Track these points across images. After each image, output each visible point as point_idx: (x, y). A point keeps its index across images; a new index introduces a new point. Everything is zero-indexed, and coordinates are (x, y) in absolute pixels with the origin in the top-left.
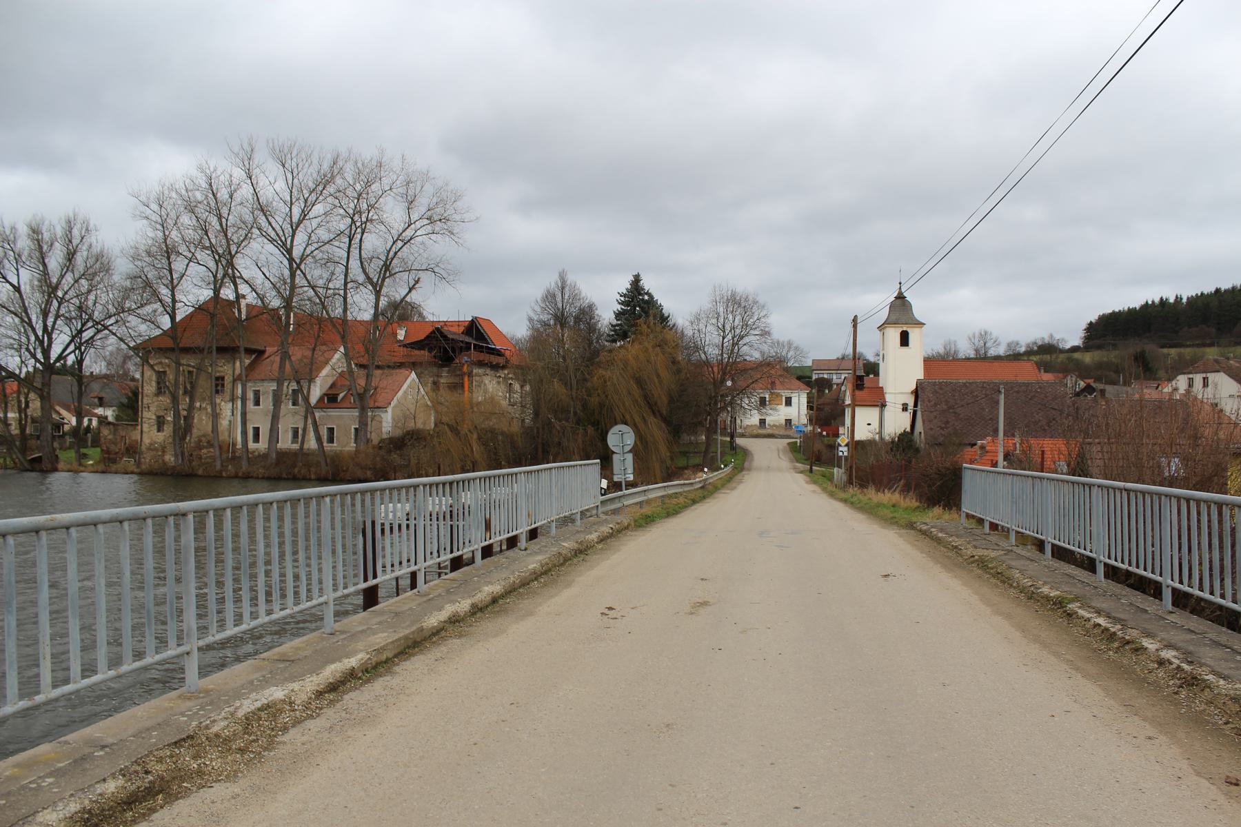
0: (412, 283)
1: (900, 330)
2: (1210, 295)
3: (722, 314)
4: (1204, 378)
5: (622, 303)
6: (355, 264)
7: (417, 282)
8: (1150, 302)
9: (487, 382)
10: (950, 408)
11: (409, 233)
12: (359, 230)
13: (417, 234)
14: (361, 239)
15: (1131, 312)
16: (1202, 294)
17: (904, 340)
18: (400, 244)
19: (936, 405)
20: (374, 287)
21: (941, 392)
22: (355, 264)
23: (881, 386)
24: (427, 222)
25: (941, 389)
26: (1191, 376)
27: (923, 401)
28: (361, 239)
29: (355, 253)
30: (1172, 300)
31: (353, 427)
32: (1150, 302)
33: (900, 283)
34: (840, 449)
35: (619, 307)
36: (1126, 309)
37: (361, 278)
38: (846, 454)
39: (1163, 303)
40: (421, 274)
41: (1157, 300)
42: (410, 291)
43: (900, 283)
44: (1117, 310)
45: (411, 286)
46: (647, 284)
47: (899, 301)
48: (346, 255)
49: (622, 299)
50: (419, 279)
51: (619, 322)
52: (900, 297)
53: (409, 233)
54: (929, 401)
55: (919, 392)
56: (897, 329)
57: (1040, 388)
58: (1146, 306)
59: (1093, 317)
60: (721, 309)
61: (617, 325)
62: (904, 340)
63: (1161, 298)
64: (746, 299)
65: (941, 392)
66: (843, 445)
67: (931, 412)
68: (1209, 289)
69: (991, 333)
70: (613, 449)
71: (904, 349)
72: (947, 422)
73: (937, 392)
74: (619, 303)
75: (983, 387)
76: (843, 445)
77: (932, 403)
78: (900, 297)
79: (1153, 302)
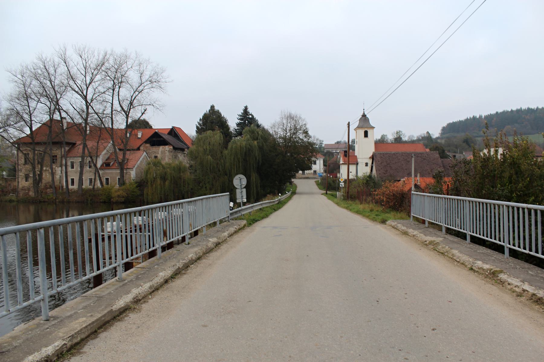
0: (143, 111)
1: (364, 130)
3: (285, 123)
5: (240, 119)
6: (116, 103)
7: (145, 110)
8: (469, 118)
9: (179, 156)
10: (388, 164)
11: (141, 88)
12: (117, 87)
13: (145, 88)
14: (119, 91)
15: (460, 122)
17: (366, 135)
18: (137, 93)
19: (381, 163)
20: (126, 114)
21: (384, 157)
22: (116, 103)
23: (356, 155)
24: (149, 82)
25: (384, 156)
27: (376, 161)
28: (119, 91)
29: (116, 98)
30: (478, 117)
31: (118, 177)
32: (469, 118)
34: (341, 184)
35: (239, 121)
36: (458, 120)
37: (119, 109)
38: (343, 186)
39: (474, 118)
40: (147, 107)
41: (472, 117)
42: (142, 114)
44: (455, 121)
45: (143, 112)
46: (250, 110)
47: (364, 118)
48: (111, 98)
49: (240, 117)
50: (146, 109)
51: (238, 128)
52: (364, 116)
53: (141, 88)
54: (379, 161)
55: (374, 158)
57: (427, 155)
58: (467, 120)
59: (445, 125)
60: (285, 121)
61: (238, 129)
62: (366, 135)
63: (474, 116)
64: (296, 117)
65: (384, 157)
66: (342, 182)
67: (380, 166)
68: (493, 112)
69: (402, 132)
70: (236, 186)
71: (366, 139)
72: (387, 171)
73: (382, 157)
74: (238, 119)
75: (402, 155)
77: (380, 162)
78: (364, 116)
79: (470, 118)
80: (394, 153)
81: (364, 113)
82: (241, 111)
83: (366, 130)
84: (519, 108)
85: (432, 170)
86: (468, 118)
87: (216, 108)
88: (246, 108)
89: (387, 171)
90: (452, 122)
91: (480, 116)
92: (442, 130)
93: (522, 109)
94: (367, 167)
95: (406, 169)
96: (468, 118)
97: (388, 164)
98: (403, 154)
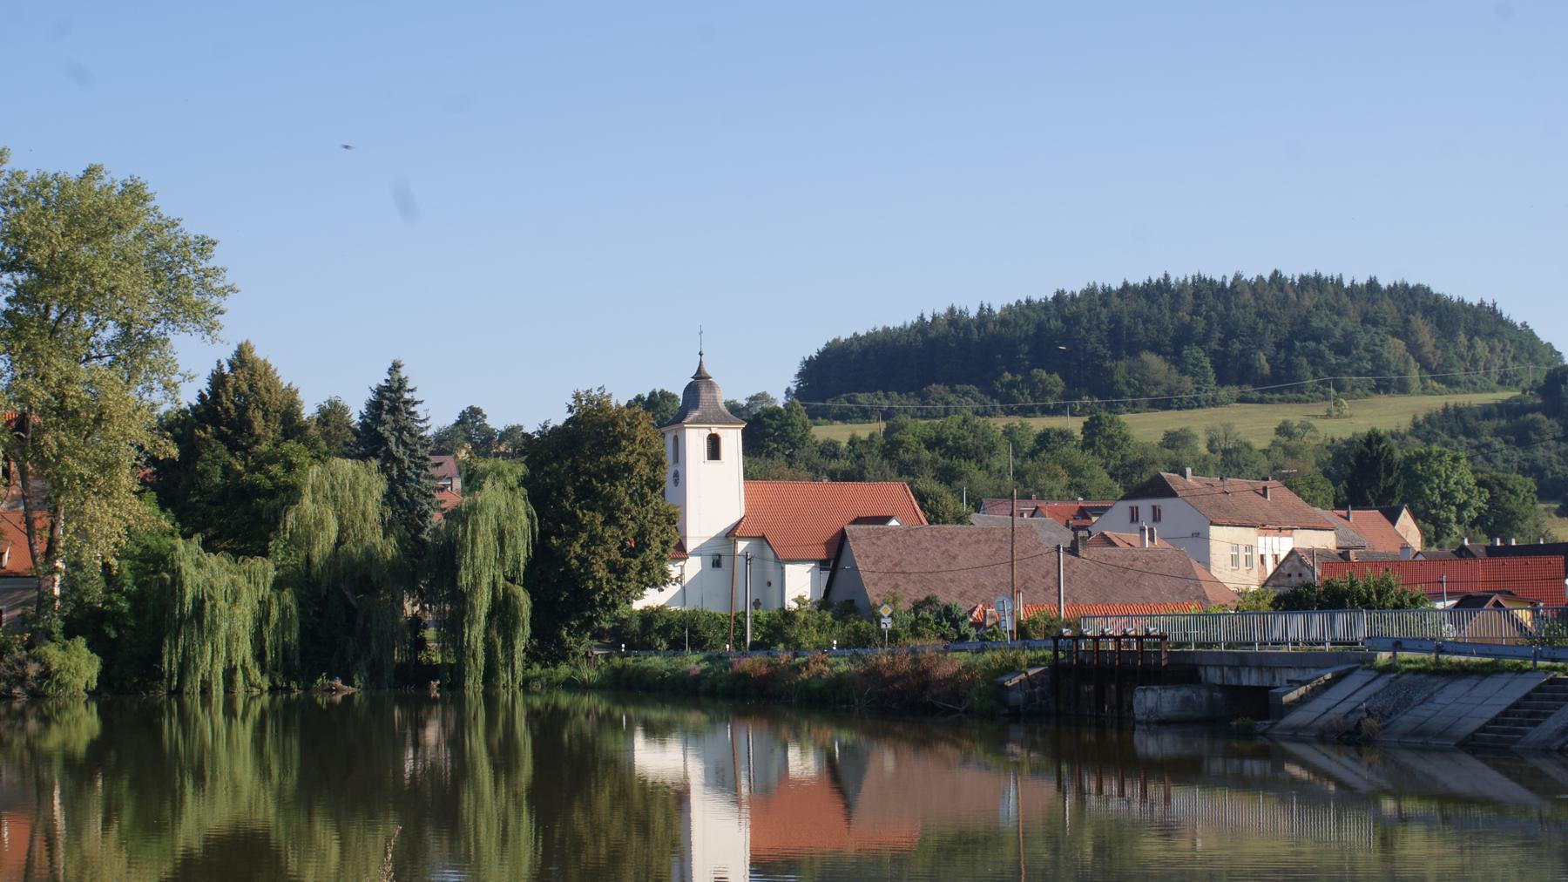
1: (707, 433)
2: (1045, 306)
4: (1154, 507)
8: (929, 319)
10: (896, 565)
16: (1028, 301)
19: (875, 563)
21: (879, 543)
26: (1134, 503)
30: (973, 313)
32: (929, 319)
33: (701, 354)
34: (883, 621)
36: (880, 329)
39: (954, 319)
41: (942, 310)
43: (701, 354)
44: (862, 333)
52: (700, 376)
54: (868, 557)
58: (921, 327)
59: (813, 348)
63: (952, 310)
65: (879, 543)
66: (886, 615)
68: (1042, 292)
73: (874, 544)
75: (932, 536)
76: (886, 615)
77: (872, 559)
82: (381, 378)
83: (714, 431)
84: (1156, 276)
85: (1026, 582)
86: (922, 318)
87: (260, 353)
88: (395, 367)
91: (982, 308)
92: (800, 375)
93: (1172, 281)
94: (717, 571)
95: (952, 581)
96: (922, 318)
97: (896, 565)
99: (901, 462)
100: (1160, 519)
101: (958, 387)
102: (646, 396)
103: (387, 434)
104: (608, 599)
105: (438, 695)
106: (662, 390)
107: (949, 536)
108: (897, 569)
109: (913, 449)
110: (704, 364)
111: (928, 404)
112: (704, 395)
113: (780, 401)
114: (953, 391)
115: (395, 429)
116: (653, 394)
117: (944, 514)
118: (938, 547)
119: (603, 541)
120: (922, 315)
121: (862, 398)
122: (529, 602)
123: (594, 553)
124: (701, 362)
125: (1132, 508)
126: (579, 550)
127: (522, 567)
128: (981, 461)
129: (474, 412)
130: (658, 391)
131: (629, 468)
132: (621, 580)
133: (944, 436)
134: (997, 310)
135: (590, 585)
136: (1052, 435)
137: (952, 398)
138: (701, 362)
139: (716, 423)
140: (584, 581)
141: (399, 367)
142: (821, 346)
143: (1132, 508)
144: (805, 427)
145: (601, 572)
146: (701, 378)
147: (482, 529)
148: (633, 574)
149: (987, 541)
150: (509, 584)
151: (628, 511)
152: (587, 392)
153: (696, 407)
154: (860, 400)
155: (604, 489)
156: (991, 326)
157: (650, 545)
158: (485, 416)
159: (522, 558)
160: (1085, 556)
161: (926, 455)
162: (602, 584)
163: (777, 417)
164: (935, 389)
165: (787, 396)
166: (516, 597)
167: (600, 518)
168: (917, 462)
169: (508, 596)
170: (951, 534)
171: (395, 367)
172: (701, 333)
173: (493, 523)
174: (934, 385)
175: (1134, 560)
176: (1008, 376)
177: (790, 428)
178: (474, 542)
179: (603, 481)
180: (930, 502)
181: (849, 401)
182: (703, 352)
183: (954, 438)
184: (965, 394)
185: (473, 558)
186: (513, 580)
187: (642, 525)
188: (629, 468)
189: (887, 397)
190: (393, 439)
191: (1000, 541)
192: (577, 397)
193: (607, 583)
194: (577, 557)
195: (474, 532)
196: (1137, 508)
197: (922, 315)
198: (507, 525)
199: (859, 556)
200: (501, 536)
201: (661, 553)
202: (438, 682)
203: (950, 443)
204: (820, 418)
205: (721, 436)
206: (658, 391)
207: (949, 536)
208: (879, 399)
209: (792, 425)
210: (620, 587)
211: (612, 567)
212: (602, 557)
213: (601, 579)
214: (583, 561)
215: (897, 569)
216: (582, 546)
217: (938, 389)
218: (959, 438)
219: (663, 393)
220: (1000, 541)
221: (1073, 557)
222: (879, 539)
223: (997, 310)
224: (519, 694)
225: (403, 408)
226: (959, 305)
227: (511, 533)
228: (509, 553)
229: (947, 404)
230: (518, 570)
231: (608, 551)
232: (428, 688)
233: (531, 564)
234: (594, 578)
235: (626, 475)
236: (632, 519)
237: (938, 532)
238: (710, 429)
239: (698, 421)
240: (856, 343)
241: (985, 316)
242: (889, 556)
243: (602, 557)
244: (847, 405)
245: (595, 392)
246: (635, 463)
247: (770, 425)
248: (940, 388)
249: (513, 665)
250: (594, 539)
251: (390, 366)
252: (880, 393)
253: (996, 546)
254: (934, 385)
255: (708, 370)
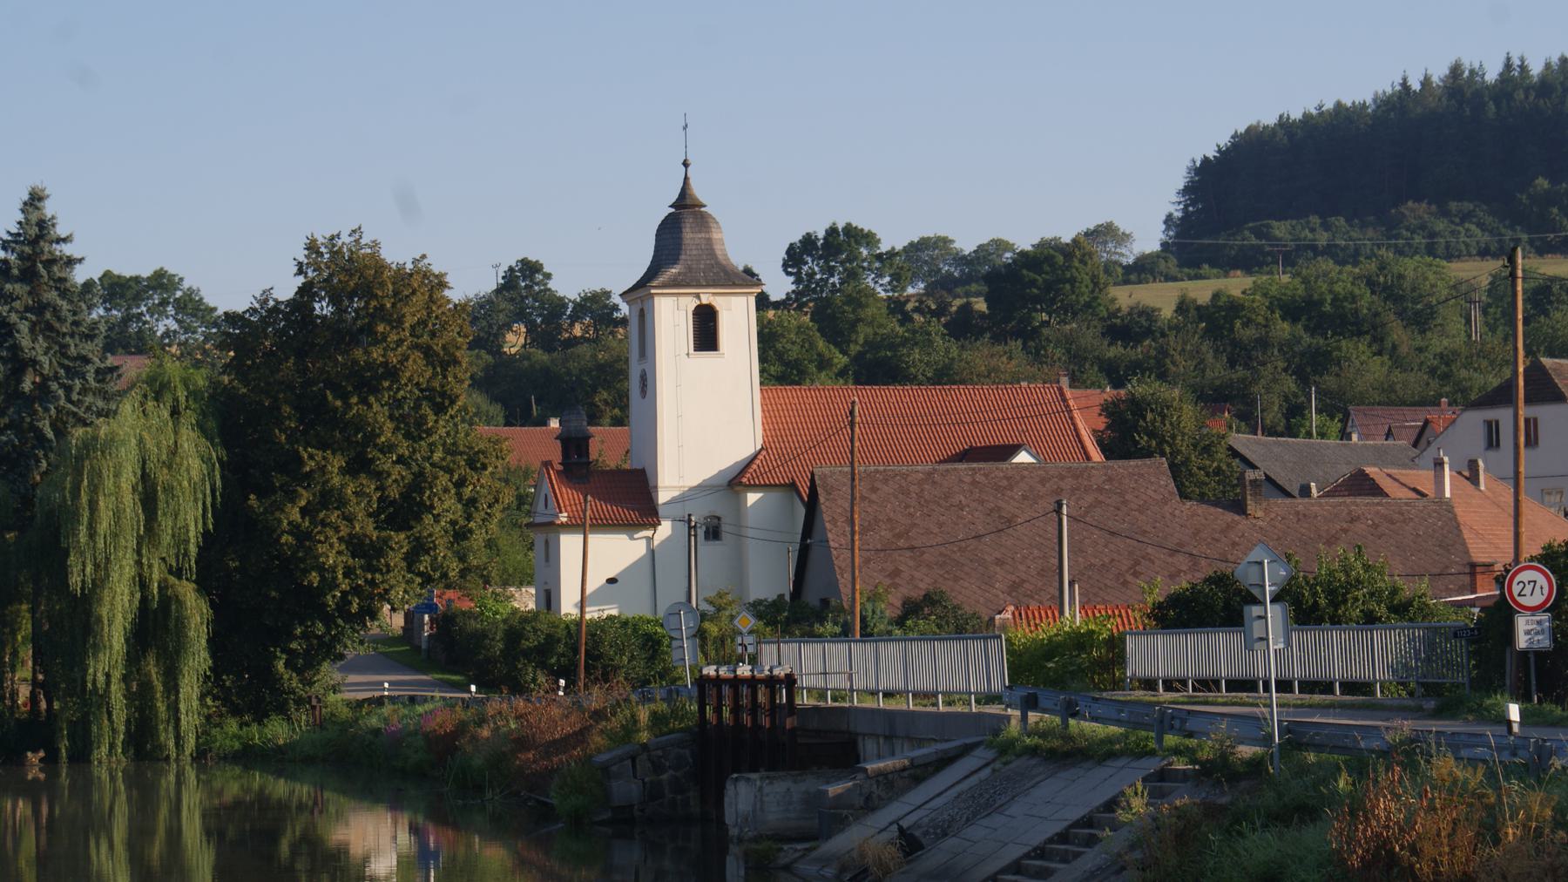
1: (692, 304)
8: (1416, 86)
10: (899, 536)
17: (706, 333)
21: (874, 497)
25: (874, 490)
30: (1492, 75)
32: (1416, 86)
33: (686, 164)
36: (1329, 105)
39: (1460, 84)
41: (1439, 73)
43: (686, 164)
44: (1296, 115)
46: (62, 213)
52: (686, 206)
56: (683, 300)
59: (1210, 140)
62: (706, 333)
63: (1456, 70)
65: (874, 497)
71: (706, 358)
75: (974, 483)
78: (686, 206)
80: (929, 474)
81: (685, 191)
83: (705, 300)
85: (1137, 563)
86: (1404, 84)
88: (35, 199)
89: (896, 573)
90: (1270, 120)
91: (1508, 65)
92: (1187, 190)
95: (999, 562)
96: (1404, 84)
97: (899, 536)
98: (979, 478)
99: (1235, 343)
100: (1498, 445)
101: (1453, 206)
102: (821, 234)
103: (14, 317)
104: (351, 603)
105: (42, 776)
106: (849, 225)
107: (1005, 483)
108: (901, 543)
109: (1260, 319)
110: (693, 183)
111: (1397, 237)
112: (689, 235)
113: (1147, 237)
114: (1445, 213)
115: (28, 309)
116: (832, 232)
117: (1174, 437)
118: (982, 502)
119: (342, 503)
120: (1405, 80)
121: (1281, 229)
122: (205, 607)
123: (324, 524)
124: (686, 178)
125: (1489, 424)
126: (295, 515)
127: (193, 550)
128: (1382, 340)
129: (530, 269)
130: (840, 226)
131: (392, 373)
132: (374, 570)
133: (1316, 297)
134: (1536, 69)
135: (314, 578)
136: (1556, 288)
137: (1440, 225)
138: (686, 178)
139: (708, 286)
140: (306, 572)
141: (41, 199)
142: (1224, 140)
143: (1489, 424)
144: (1096, 284)
145: (332, 555)
146: (685, 207)
147: (109, 484)
148: (395, 559)
149: (1073, 490)
150: (172, 580)
151: (388, 449)
152: (332, 238)
153: (674, 260)
154: (1277, 232)
155: (348, 406)
156: (1520, 95)
157: (432, 507)
158: (548, 276)
159: (192, 534)
160: (1260, 514)
161: (1283, 329)
162: (335, 578)
163: (1047, 268)
164: (1412, 210)
165: (1168, 228)
166: (180, 603)
167: (336, 463)
168: (1263, 343)
169: (168, 600)
170: (1008, 478)
171: (35, 199)
172: (685, 127)
173: (129, 477)
174: (1410, 204)
175: (1352, 521)
176: (1542, 183)
177: (1068, 286)
178: (93, 506)
179: (345, 397)
180: (1149, 416)
181: (1259, 234)
182: (690, 160)
183: (1334, 300)
184: (1465, 217)
185: (92, 534)
186: (178, 573)
187: (420, 475)
188: (392, 373)
189: (1326, 227)
190: (24, 327)
191: (1100, 490)
192: (312, 247)
193: (346, 575)
194: (295, 529)
195: (94, 489)
196: (1497, 423)
197: (1405, 80)
198: (162, 476)
199: (834, 521)
200: (149, 498)
201: (462, 522)
202: (42, 754)
203: (1327, 308)
204: (1206, 266)
205: (718, 308)
206: (840, 226)
207: (1005, 483)
208: (1312, 230)
209: (1072, 281)
210: (372, 583)
211: (356, 546)
212: (337, 530)
213: (333, 569)
214: (303, 537)
215: (901, 543)
216: (304, 512)
217: (1415, 211)
218: (1345, 299)
219: (850, 230)
220: (1100, 490)
221: (1237, 517)
222: (874, 490)
223: (1536, 69)
224: (191, 775)
225: (43, 272)
226: (1469, 61)
227: (169, 489)
228: (166, 524)
229: (1433, 235)
230: (186, 554)
231: (350, 519)
232: (21, 762)
233: (209, 540)
234: (321, 569)
235: (386, 384)
236: (400, 460)
237: (986, 475)
238: (698, 296)
239: (675, 283)
240: (1280, 133)
241: (1513, 76)
242: (890, 520)
243: (337, 530)
244: (1254, 241)
245: (346, 238)
246: (401, 362)
247: (1033, 283)
248: (1422, 207)
249: (178, 720)
250: (329, 498)
251: (26, 197)
252: (1315, 220)
253: (1089, 499)
254: (1410, 204)
255: (699, 191)
